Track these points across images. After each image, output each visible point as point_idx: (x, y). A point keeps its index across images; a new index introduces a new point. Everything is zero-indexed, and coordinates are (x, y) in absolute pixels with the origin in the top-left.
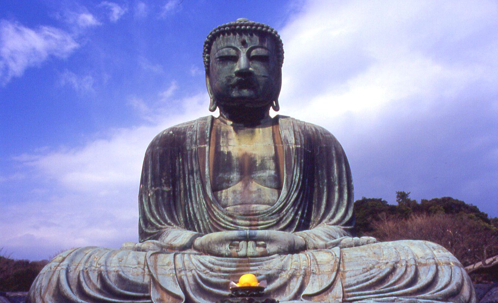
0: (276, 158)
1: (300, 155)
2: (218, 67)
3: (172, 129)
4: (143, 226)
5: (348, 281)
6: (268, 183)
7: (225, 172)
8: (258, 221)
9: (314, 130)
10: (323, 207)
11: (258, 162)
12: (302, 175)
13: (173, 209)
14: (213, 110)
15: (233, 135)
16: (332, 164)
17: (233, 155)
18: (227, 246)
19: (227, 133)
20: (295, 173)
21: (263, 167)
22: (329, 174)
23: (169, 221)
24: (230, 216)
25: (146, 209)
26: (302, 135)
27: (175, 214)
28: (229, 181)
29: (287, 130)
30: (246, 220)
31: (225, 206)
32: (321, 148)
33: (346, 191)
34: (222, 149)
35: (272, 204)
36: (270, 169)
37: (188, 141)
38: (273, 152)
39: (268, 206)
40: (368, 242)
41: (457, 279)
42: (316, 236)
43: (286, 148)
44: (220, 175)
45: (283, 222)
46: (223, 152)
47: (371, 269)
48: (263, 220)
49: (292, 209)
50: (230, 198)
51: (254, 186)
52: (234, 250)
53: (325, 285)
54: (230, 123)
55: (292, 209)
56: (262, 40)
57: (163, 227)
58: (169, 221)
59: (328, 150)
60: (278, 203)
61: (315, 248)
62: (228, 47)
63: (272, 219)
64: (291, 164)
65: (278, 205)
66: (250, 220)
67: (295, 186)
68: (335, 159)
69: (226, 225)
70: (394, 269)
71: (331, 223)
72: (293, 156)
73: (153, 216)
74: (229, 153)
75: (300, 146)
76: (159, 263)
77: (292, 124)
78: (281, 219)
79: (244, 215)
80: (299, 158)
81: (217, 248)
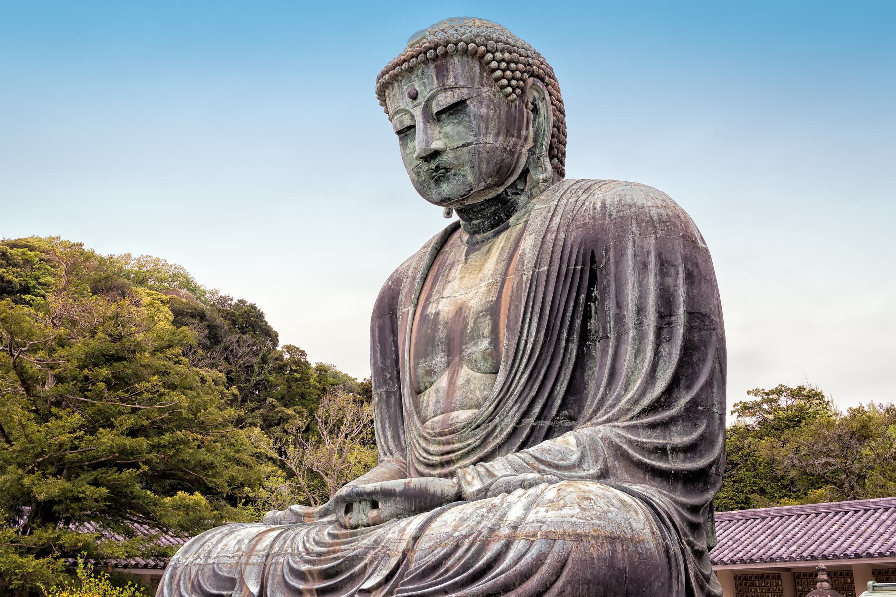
0: (493, 310)
1: (541, 289)
7: (426, 355)
8: (454, 444)
9: (599, 209)
11: (470, 326)
12: (543, 332)
13: (400, 423)
14: (449, 214)
17: (440, 318)
18: (343, 511)
19: (453, 265)
20: (525, 335)
21: (476, 337)
23: (392, 447)
24: (425, 439)
26: (562, 236)
27: (401, 432)
28: (430, 372)
29: (533, 236)
30: (439, 443)
31: (423, 422)
34: (429, 311)
35: (478, 406)
36: (484, 337)
38: (494, 299)
39: (475, 411)
42: (488, 470)
45: (496, 437)
46: (427, 315)
47: (436, 548)
48: (460, 441)
49: (516, 408)
50: (431, 404)
52: (349, 515)
55: (516, 408)
56: (442, 72)
57: (386, 458)
58: (392, 447)
60: (487, 403)
62: (397, 113)
63: (474, 435)
64: (517, 316)
66: (443, 444)
67: (525, 360)
68: (630, 268)
69: (420, 455)
70: (457, 547)
71: (605, 418)
74: (437, 314)
75: (545, 268)
76: (259, 547)
77: (550, 214)
78: (489, 435)
79: (441, 434)
80: (540, 297)
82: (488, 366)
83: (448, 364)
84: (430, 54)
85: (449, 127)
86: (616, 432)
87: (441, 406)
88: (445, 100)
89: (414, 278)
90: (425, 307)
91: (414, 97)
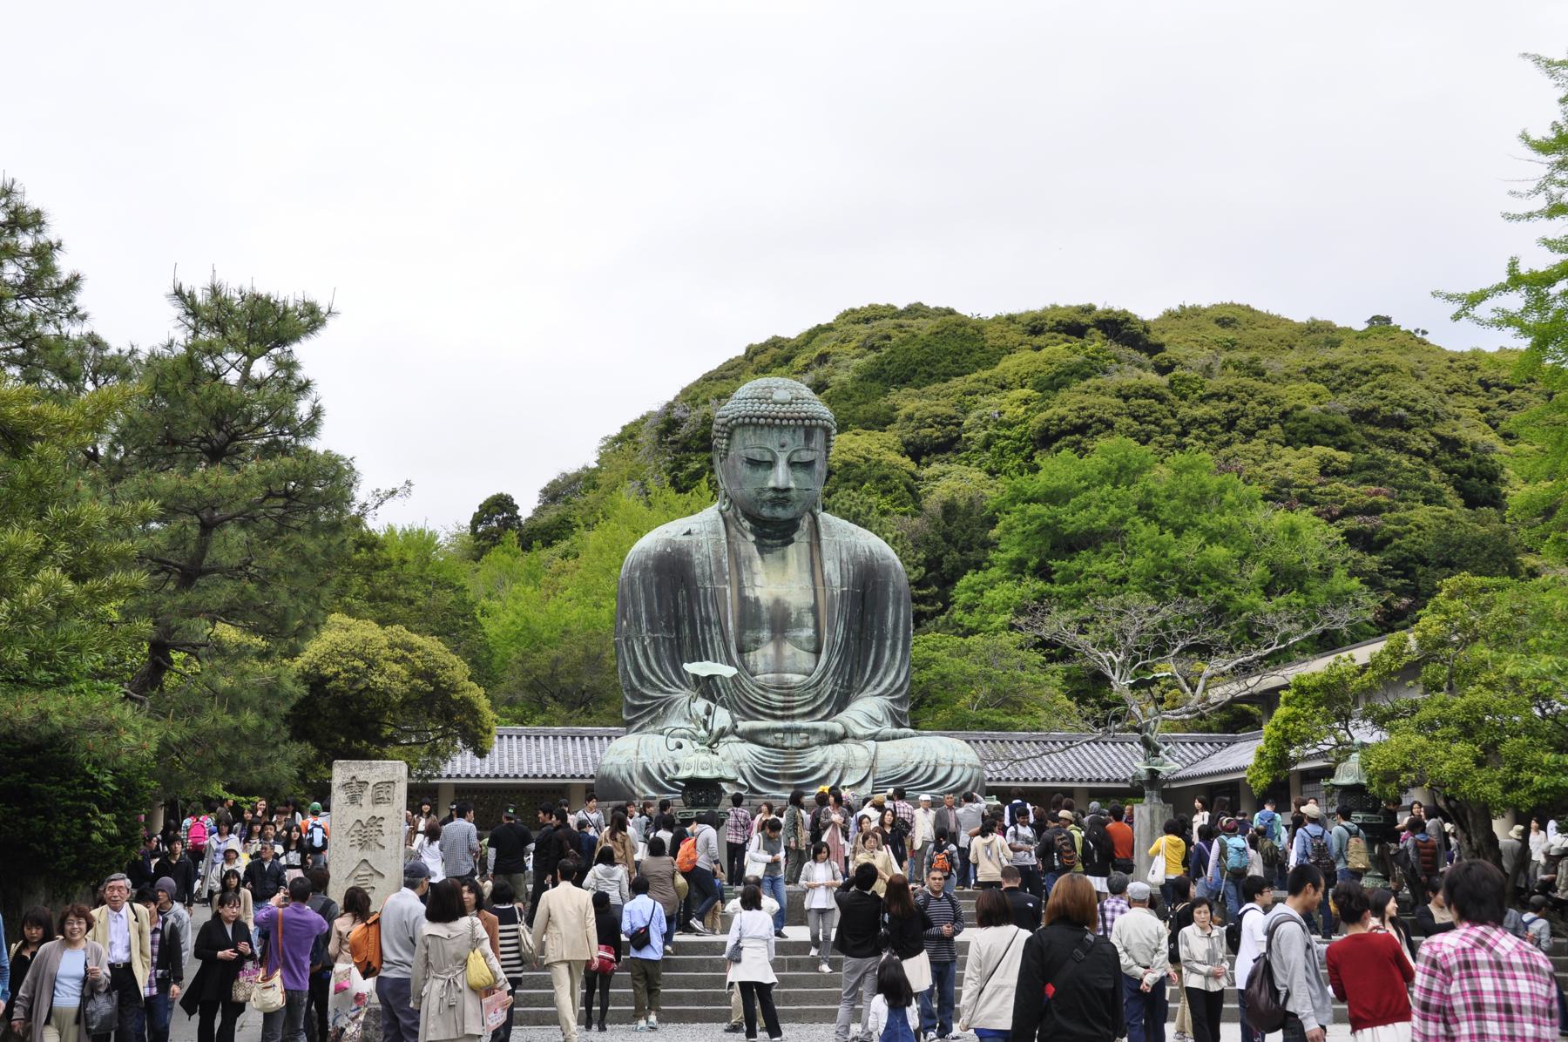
2: (745, 471)
3: (670, 542)
4: (636, 683)
5: (877, 776)
6: (806, 645)
7: (753, 629)
10: (869, 669)
11: (794, 616)
15: (758, 563)
16: (887, 608)
19: (750, 560)
21: (800, 625)
22: (883, 621)
25: (641, 661)
28: (757, 641)
31: (753, 674)
32: (875, 583)
33: (900, 646)
37: (698, 571)
40: (905, 736)
41: (964, 779)
43: (828, 593)
44: (748, 633)
51: (788, 649)
53: (860, 779)
54: (752, 538)
59: (886, 585)
61: (855, 737)
65: (816, 676)
70: (916, 768)
72: (837, 606)
73: (653, 673)
74: (757, 599)
81: (763, 738)
82: (812, 647)
83: (772, 639)
84: (807, 422)
85: (801, 475)
86: (884, 701)
87: (771, 668)
88: (806, 456)
89: (719, 562)
90: (741, 588)
91: (783, 446)
